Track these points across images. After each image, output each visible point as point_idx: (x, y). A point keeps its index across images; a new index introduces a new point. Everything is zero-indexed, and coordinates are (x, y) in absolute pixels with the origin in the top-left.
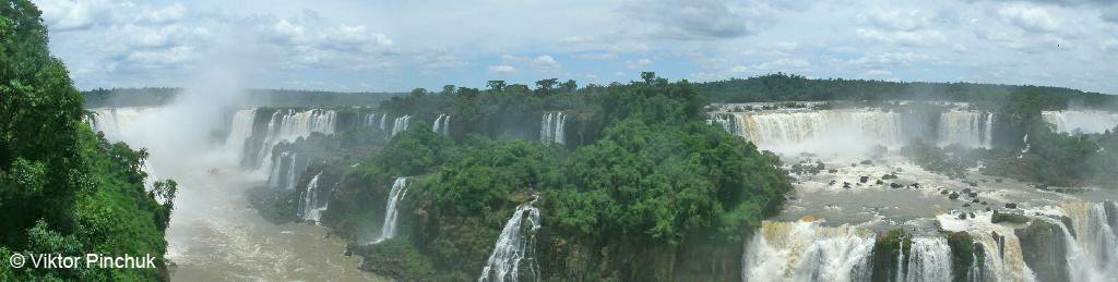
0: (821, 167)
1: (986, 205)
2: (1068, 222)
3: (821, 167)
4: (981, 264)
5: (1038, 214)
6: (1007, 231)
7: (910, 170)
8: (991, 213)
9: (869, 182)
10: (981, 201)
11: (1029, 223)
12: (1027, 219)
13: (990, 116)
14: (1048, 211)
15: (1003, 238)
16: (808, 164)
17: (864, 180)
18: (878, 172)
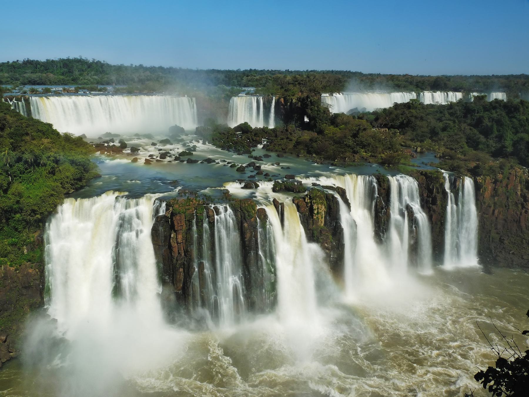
0: (124, 146)
1: (267, 177)
2: (342, 192)
3: (124, 146)
4: (264, 226)
5: (314, 184)
6: (286, 199)
7: (203, 148)
8: (273, 183)
9: (168, 159)
10: (264, 173)
11: (306, 193)
12: (305, 189)
13: (274, 98)
14: (324, 181)
15: (282, 204)
16: (111, 144)
17: (164, 156)
18: (178, 149)
